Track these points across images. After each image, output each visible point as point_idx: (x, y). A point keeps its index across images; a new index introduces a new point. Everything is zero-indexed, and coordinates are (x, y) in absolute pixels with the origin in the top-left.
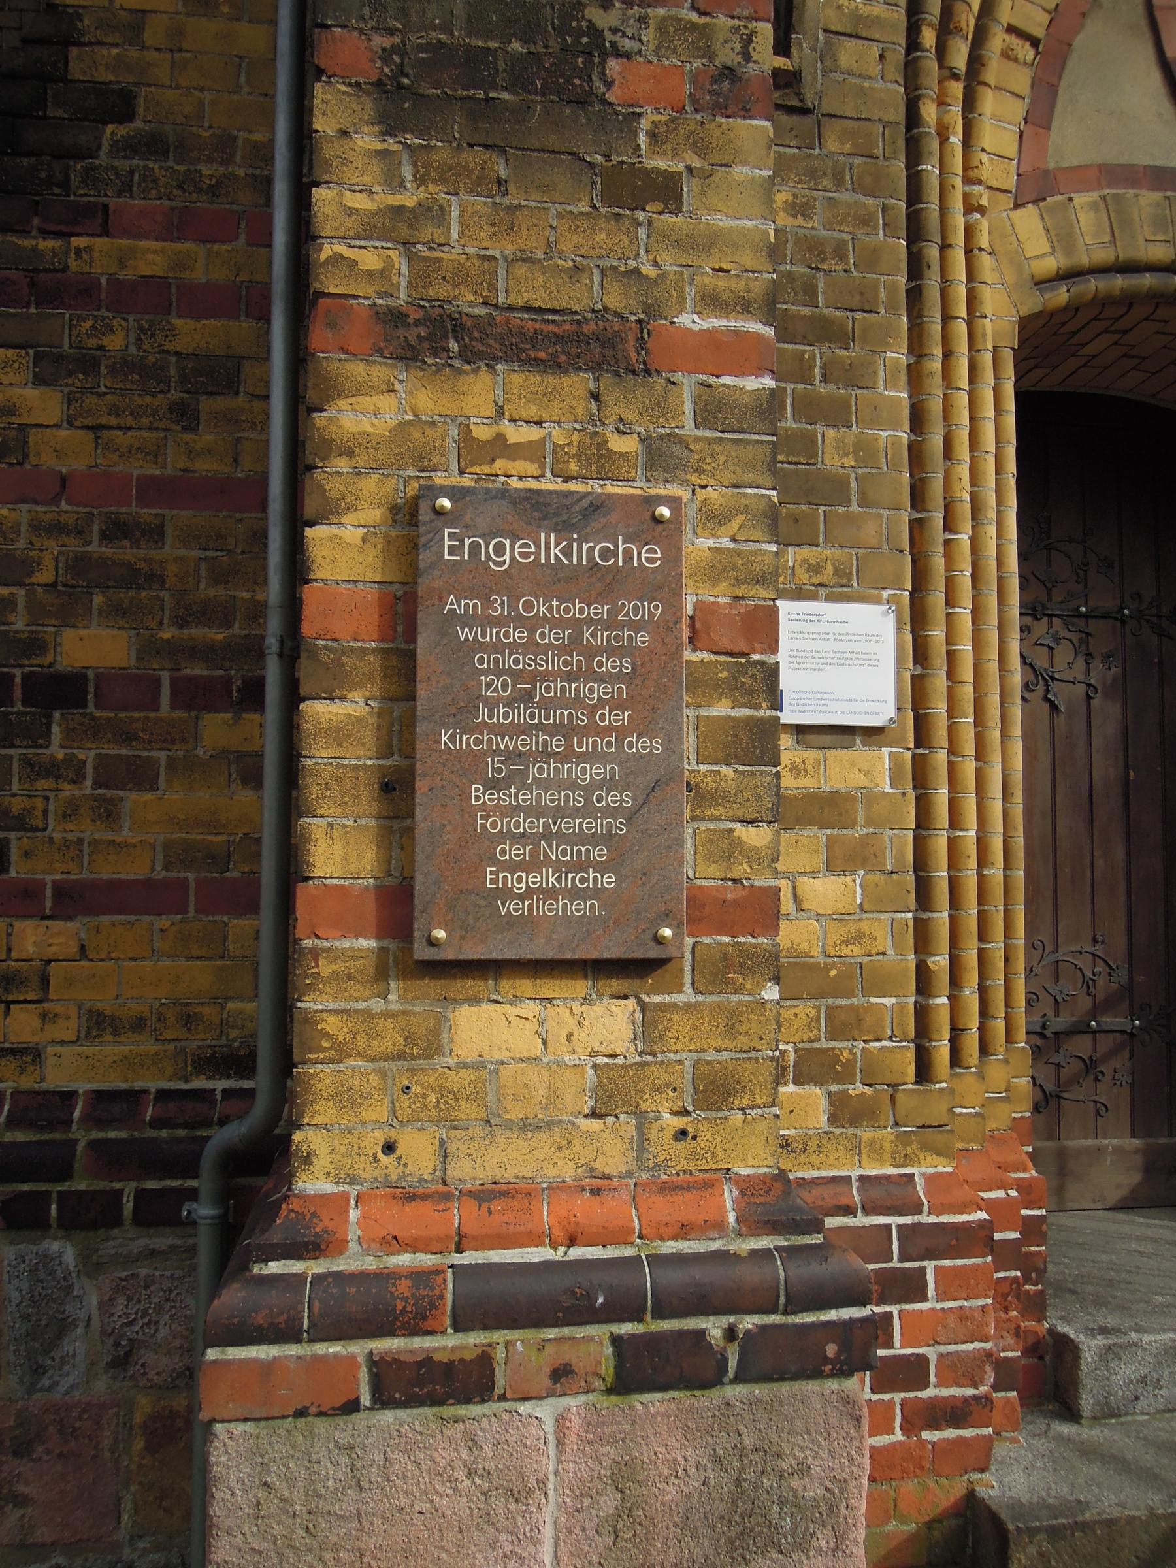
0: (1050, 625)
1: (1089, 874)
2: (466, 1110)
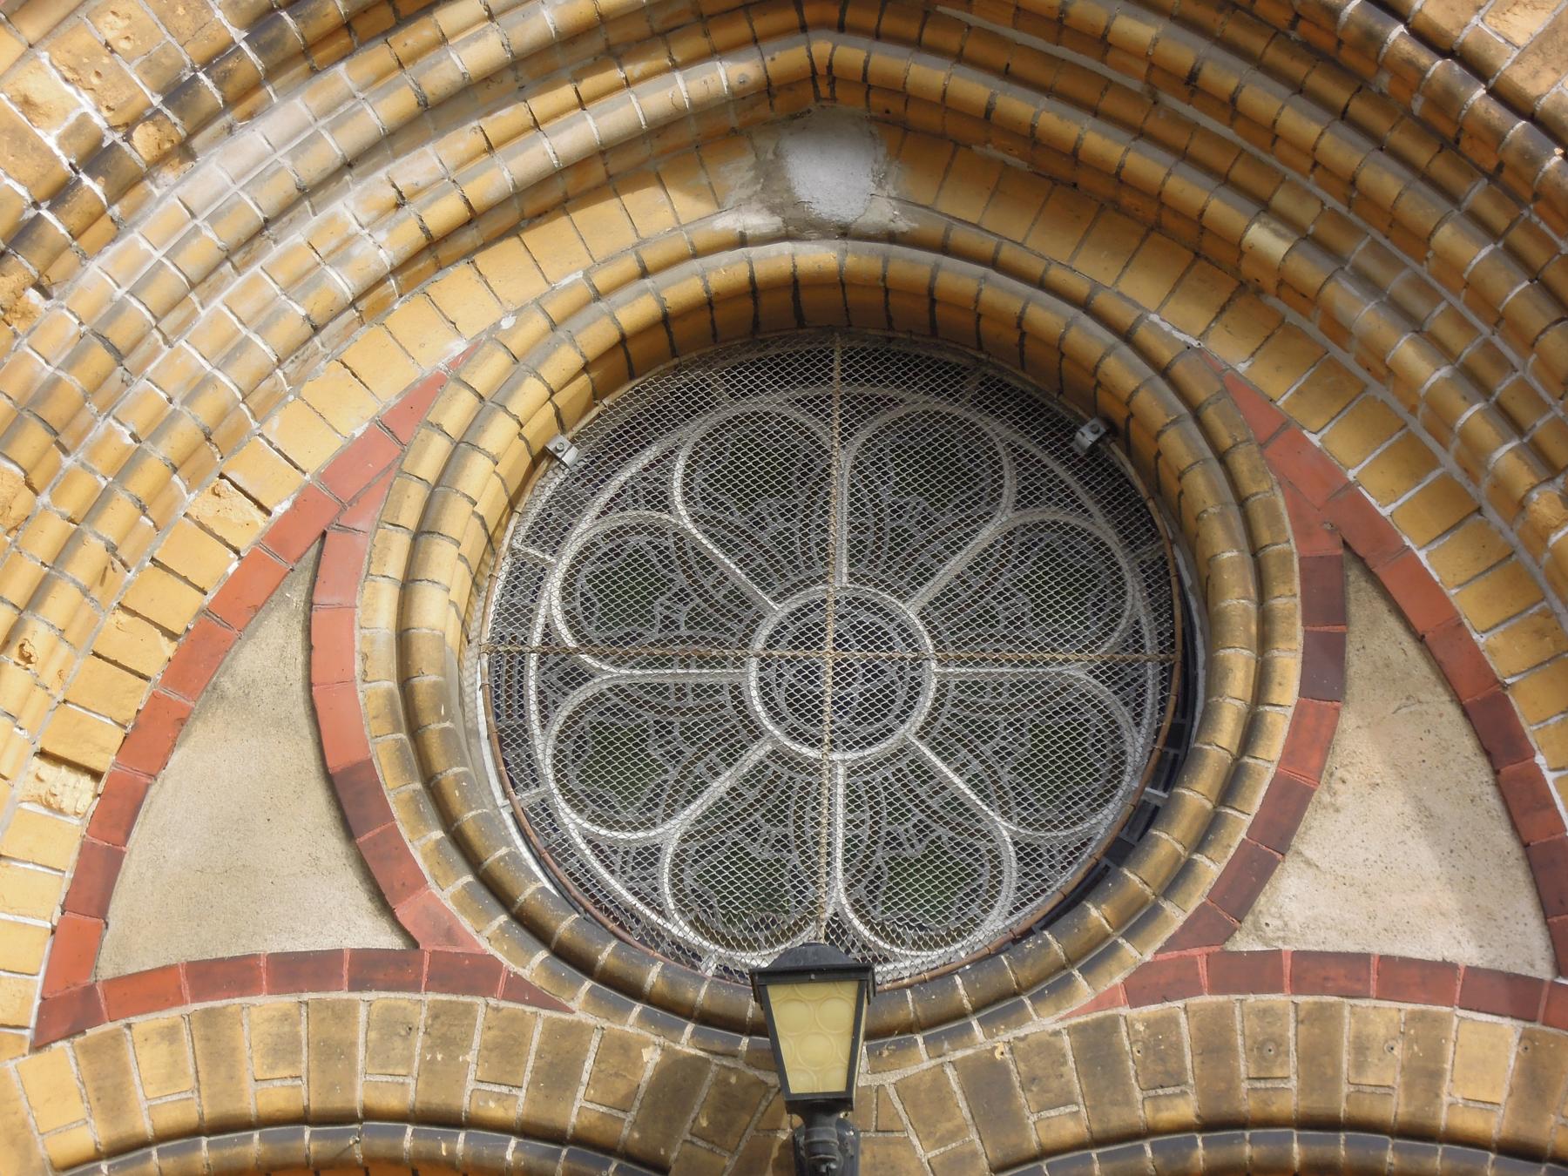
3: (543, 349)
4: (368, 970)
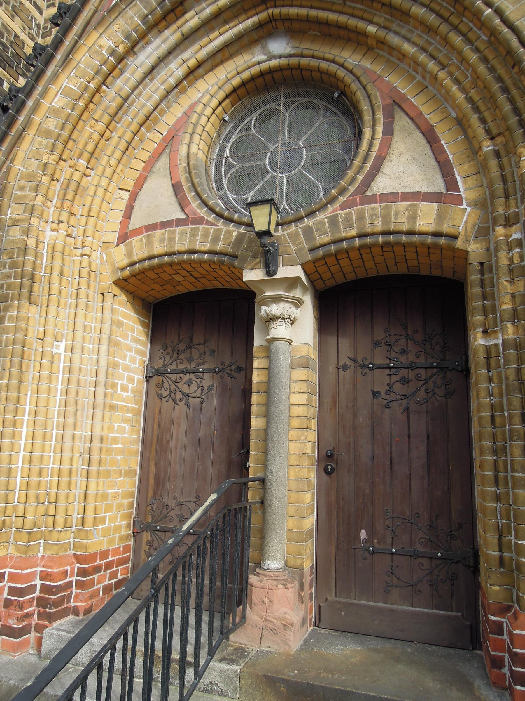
0: (190, 376)
1: (196, 471)
3: (216, 92)
4: (179, 222)
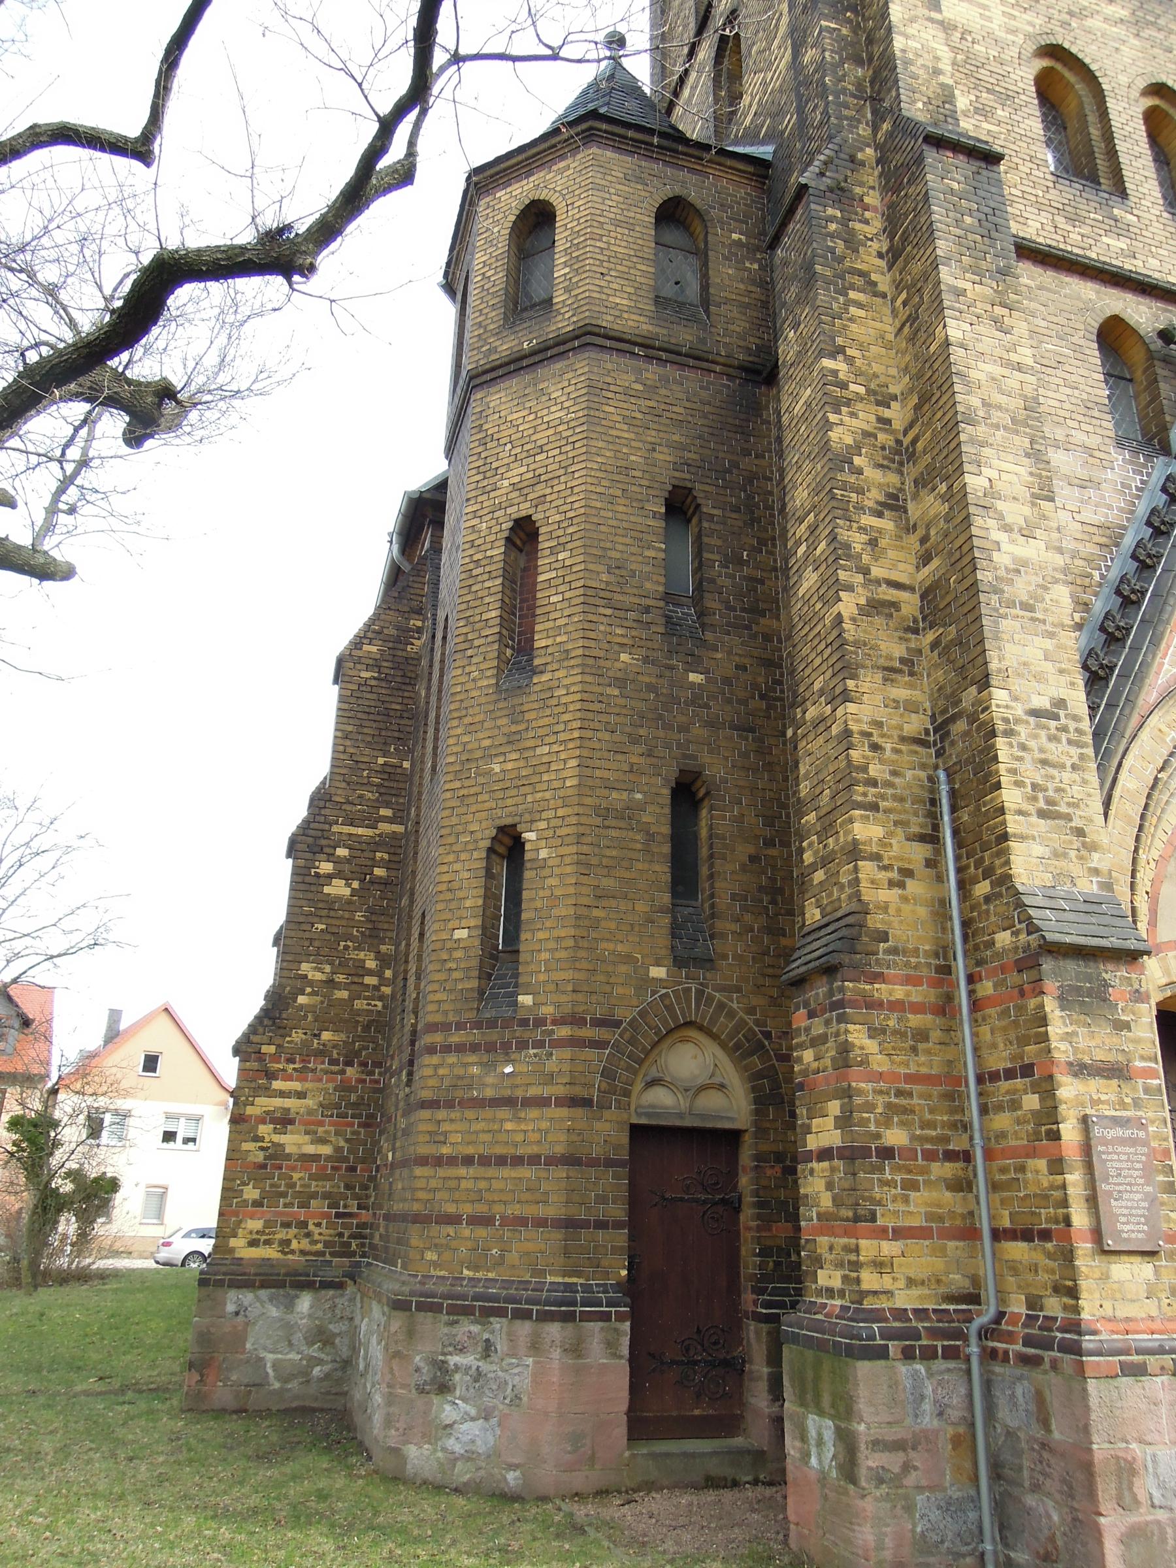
2: (1118, 1296)
